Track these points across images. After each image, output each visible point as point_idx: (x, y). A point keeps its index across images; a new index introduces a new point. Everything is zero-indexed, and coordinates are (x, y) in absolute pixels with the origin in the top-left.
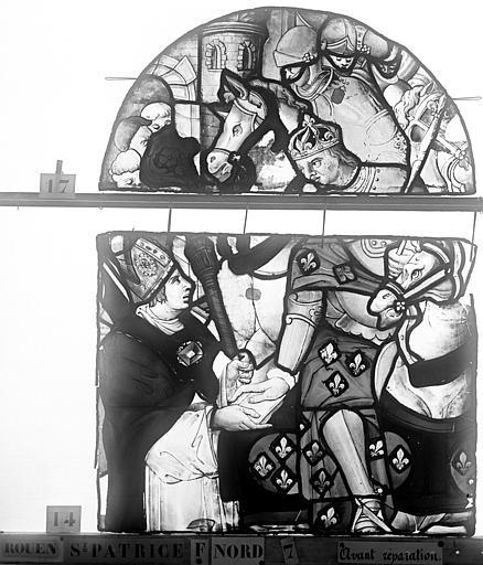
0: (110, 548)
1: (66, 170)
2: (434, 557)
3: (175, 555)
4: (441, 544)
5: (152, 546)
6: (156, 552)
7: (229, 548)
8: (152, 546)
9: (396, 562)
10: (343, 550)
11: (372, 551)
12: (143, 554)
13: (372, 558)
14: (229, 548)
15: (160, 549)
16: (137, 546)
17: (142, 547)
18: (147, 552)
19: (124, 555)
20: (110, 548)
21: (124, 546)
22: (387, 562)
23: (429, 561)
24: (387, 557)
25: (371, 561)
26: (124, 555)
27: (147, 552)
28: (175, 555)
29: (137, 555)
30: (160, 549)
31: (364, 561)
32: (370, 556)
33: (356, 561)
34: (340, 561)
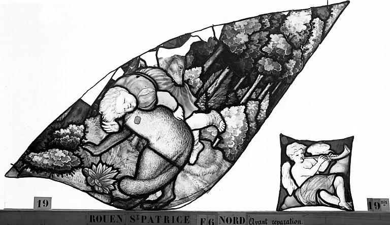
3: (186, 222)
5: (173, 217)
6: (175, 220)
7: (227, 219)
8: (173, 217)
11: (266, 220)
12: (168, 221)
13: (266, 223)
14: (227, 219)
16: (165, 217)
17: (168, 218)
19: (158, 222)
20: (151, 218)
21: (158, 217)
26: (158, 222)
27: (171, 219)
28: (186, 222)
29: (165, 222)
32: (265, 222)
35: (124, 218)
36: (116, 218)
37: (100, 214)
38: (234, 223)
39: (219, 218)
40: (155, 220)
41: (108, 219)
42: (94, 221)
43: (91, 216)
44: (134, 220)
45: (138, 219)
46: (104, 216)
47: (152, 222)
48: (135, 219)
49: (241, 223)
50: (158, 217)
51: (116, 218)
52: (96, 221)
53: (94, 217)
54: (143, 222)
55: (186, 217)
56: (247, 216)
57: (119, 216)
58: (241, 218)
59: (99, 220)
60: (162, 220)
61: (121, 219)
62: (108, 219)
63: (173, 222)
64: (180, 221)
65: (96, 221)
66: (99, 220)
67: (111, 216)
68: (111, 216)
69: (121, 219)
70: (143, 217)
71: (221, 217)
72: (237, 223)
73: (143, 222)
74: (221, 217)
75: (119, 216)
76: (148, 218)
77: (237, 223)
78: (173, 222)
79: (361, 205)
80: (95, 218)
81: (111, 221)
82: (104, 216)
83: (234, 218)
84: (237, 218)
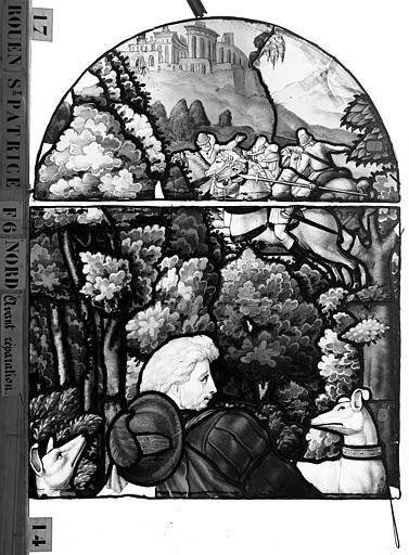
0: (16, 117)
2: (9, 387)
3: (8, 180)
5: (18, 158)
8: (18, 158)
9: (3, 351)
10: (13, 298)
11: (12, 327)
12: (11, 149)
15: (17, 166)
16: (18, 143)
17: (17, 148)
18: (13, 153)
19: (9, 130)
20: (16, 117)
21: (18, 131)
22: (3, 342)
23: (4, 383)
24: (8, 341)
25: (3, 326)
26: (9, 130)
27: (11, 153)
28: (8, 180)
29: (9, 143)
30: (17, 166)
31: (3, 320)
32: (9, 324)
33: (3, 312)
34: (3, 296)
35: (16, 67)
36: (15, 53)
37: (24, 23)
38: (7, 269)
39: (17, 241)
40: (12, 125)
41: (15, 38)
42: (10, 13)
43: (20, 8)
44: (12, 87)
45: (14, 93)
46: (19, 32)
47: (9, 120)
48: (14, 89)
49: (7, 281)
50: (18, 131)
51: (15, 53)
52: (12, 16)
53: (19, 13)
54: (9, 102)
55: (18, 180)
56: (20, 292)
57: (20, 58)
58: (17, 281)
59: (12, 22)
60: (13, 137)
61: (13, 62)
62: (15, 38)
63: (9, 157)
64: (10, 169)
65: (12, 16)
66: (12, 22)
67: (19, 45)
68: (19, 45)
69: (13, 62)
70: (19, 102)
71: (17, 245)
72: (7, 275)
73: (9, 102)
74: (17, 245)
75: (20, 58)
76: (15, 112)
77: (7, 275)
78: (9, 157)
79: (36, 509)
80: (16, 15)
81: (10, 44)
82: (19, 32)
83: (16, 269)
84: (15, 274)
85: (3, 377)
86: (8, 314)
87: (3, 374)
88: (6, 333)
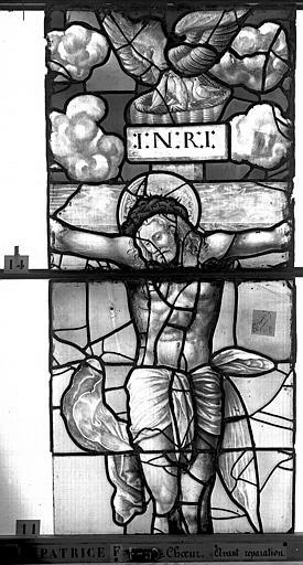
1: (21, 253)
4: (285, 544)
5: (83, 550)
6: (85, 552)
8: (83, 550)
18: (79, 552)
19: (63, 556)
24: (247, 554)
25: (235, 557)
26: (63, 556)
27: (79, 552)
34: (214, 557)
47: (55, 557)
60: (68, 554)
76: (50, 551)
85: (274, 557)
86: (228, 554)
87: (270, 557)
88: (242, 554)
